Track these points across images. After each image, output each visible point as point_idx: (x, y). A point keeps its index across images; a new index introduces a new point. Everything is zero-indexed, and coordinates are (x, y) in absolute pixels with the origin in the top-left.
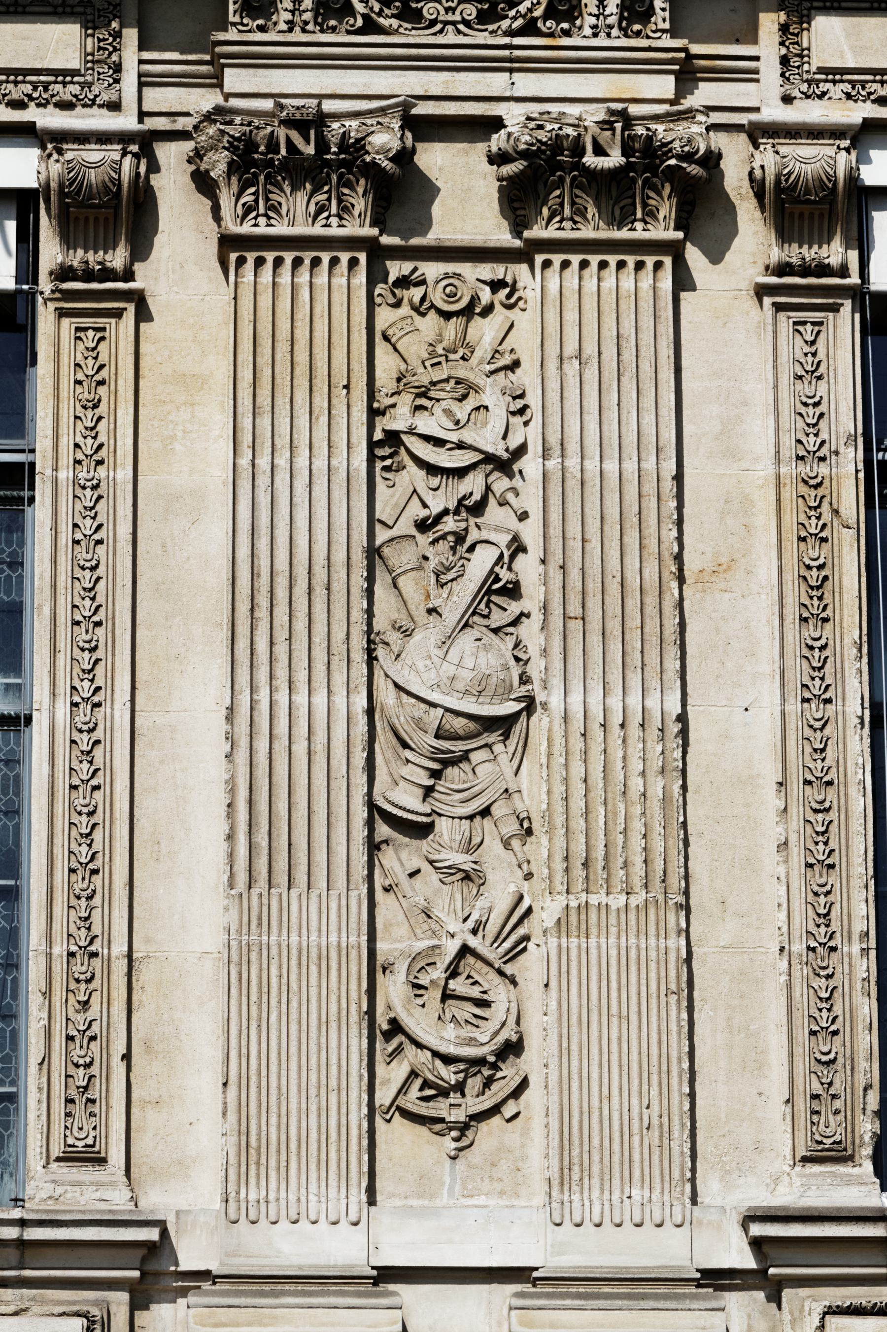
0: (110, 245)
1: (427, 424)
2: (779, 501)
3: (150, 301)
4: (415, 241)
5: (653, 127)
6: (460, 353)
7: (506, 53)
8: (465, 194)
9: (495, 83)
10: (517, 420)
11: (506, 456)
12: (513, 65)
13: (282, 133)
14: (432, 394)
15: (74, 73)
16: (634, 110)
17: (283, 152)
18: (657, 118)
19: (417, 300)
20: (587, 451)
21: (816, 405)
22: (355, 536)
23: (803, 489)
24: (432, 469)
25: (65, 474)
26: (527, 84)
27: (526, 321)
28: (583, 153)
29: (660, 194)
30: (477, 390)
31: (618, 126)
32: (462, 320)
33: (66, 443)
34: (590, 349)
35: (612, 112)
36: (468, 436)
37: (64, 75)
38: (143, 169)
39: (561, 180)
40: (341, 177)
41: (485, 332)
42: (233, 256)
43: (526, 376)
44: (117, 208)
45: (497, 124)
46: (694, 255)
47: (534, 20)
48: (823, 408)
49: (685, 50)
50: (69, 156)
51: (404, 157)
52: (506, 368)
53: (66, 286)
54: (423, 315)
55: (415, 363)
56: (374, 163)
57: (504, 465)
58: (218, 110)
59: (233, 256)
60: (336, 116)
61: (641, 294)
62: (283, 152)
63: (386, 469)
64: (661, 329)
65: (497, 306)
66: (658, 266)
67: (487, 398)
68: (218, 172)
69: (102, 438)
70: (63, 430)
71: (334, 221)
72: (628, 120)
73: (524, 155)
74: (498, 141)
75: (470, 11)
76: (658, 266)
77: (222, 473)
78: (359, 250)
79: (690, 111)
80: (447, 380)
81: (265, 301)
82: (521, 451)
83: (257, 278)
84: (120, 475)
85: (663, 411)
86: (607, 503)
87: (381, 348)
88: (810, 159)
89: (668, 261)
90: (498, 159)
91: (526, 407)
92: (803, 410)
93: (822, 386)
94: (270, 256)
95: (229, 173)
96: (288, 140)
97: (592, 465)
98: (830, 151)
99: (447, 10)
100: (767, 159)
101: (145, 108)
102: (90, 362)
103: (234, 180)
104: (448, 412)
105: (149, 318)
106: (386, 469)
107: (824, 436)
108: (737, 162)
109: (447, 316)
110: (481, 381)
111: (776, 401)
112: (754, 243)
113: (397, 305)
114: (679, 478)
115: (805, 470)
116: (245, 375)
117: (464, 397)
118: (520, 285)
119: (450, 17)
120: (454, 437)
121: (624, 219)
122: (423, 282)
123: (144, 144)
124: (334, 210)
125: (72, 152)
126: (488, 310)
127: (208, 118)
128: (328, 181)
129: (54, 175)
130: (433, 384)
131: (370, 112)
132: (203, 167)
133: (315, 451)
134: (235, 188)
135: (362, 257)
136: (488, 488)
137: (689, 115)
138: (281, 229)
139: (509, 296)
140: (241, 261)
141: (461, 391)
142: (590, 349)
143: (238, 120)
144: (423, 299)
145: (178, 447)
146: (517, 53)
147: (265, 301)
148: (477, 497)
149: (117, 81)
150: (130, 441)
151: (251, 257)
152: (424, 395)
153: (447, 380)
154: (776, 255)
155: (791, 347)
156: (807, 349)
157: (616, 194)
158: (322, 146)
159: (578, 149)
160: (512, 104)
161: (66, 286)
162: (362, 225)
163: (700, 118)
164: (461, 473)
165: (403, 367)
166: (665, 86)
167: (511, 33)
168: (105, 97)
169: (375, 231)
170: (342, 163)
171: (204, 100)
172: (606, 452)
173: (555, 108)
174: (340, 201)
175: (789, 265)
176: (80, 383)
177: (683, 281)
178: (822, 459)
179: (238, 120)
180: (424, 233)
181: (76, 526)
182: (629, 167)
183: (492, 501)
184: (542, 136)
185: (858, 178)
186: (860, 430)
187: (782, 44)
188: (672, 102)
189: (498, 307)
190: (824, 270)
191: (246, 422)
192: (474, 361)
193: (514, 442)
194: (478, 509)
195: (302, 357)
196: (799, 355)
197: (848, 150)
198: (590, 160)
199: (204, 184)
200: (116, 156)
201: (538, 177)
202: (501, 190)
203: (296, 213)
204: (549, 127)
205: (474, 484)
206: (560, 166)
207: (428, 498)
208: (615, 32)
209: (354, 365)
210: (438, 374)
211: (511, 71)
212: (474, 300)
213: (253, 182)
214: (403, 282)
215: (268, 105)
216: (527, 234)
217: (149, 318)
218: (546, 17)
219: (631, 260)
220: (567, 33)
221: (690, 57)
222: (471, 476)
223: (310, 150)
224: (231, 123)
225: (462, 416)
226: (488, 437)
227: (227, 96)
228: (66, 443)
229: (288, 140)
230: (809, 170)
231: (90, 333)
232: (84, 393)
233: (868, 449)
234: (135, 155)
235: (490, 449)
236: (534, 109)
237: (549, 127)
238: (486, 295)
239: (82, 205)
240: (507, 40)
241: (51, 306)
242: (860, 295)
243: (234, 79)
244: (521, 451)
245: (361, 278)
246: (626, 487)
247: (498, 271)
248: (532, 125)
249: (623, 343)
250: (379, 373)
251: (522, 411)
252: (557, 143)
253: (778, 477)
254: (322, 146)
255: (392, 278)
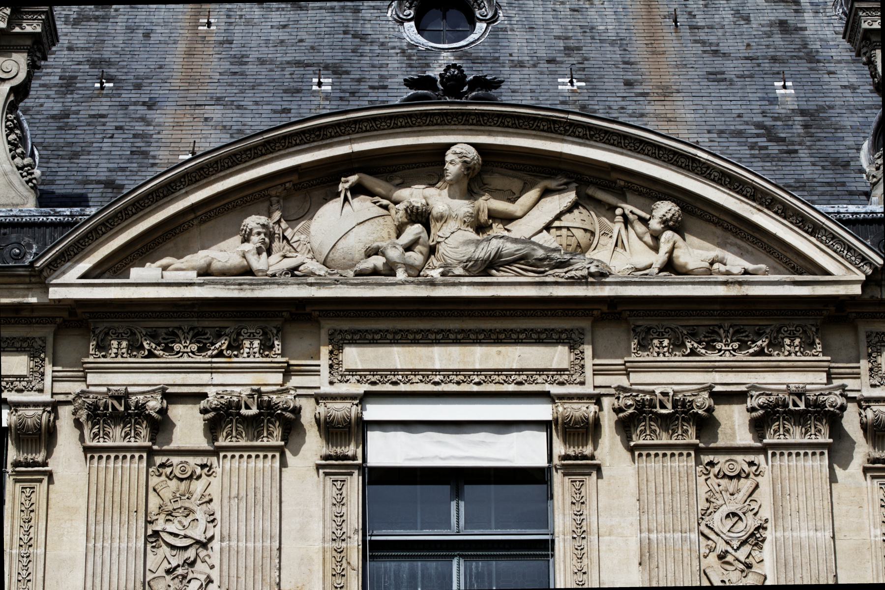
0: (38, 451)
1: (171, 528)
2: (324, 559)
3: (54, 475)
4: (165, 447)
5: (271, 396)
6: (187, 496)
7: (209, 365)
8: (188, 427)
9: (205, 378)
10: (211, 525)
11: (205, 541)
12: (212, 370)
13: (110, 402)
14: (174, 514)
15: (24, 377)
16: (263, 389)
17: (110, 410)
18: (273, 392)
19: (168, 473)
20: (240, 539)
21: (341, 516)
22: (138, 576)
23: (335, 554)
24: (173, 547)
25: (15, 551)
26: (218, 378)
27: (215, 482)
28: (241, 408)
29: (274, 426)
30: (193, 512)
31: (256, 396)
32: (188, 481)
33: (16, 537)
34: (243, 493)
35: (253, 390)
36: (188, 532)
37: (20, 378)
38: (52, 418)
39: (231, 420)
40: (136, 420)
41: (198, 487)
42: (89, 455)
43: (215, 506)
44: (40, 435)
45: (205, 396)
46: (288, 454)
47: (222, 350)
48: (344, 518)
49: (287, 362)
50: (19, 413)
51: (163, 412)
52: (206, 502)
53: (17, 469)
54: (171, 480)
55: (167, 501)
56: (149, 414)
57: (204, 545)
58: (83, 392)
59: (89, 455)
60: (134, 394)
61: (266, 469)
62: (110, 410)
63: (153, 547)
64: (274, 484)
65: (203, 475)
66: (273, 457)
67: (197, 516)
68: (83, 419)
69: (31, 535)
70: (15, 532)
71: (132, 439)
72: (260, 393)
73: (214, 409)
74: (203, 404)
75: (194, 347)
76: (273, 457)
77: (83, 550)
78: (143, 452)
79: (287, 389)
80: (180, 508)
81: (102, 475)
82: (212, 538)
83: (103, 466)
84: (39, 551)
85: (274, 520)
86: (248, 561)
87: (152, 495)
88: (340, 410)
89: (278, 455)
90: (204, 411)
91: (215, 519)
92: (335, 519)
93: (344, 509)
94: (105, 455)
95: (87, 420)
96: (112, 404)
97: (242, 544)
98: (349, 405)
99: (184, 347)
100: (322, 410)
101: (55, 391)
102: (28, 502)
103: (90, 423)
104: (180, 522)
105: (53, 483)
106: (153, 547)
107: (344, 530)
108: (309, 412)
109: (181, 480)
110: (195, 508)
111: (324, 515)
112: (314, 445)
113: (160, 475)
114: (280, 549)
115: (336, 545)
116: (93, 507)
117: (188, 515)
118: (214, 466)
119: (186, 350)
120: (182, 533)
121: (258, 436)
122: (172, 465)
123: (54, 407)
124: (133, 435)
125: (22, 411)
126: (199, 477)
127: (78, 396)
128: (130, 422)
129: (13, 421)
130: (174, 510)
131: (149, 392)
132: (77, 417)
133: (122, 540)
134: (90, 426)
135: (145, 455)
136: (197, 554)
137: (286, 391)
138: (109, 443)
139: (209, 471)
140: (92, 457)
141: (187, 512)
142: (243, 493)
143: (91, 396)
144: (171, 473)
145: (65, 538)
146: (214, 365)
147: (102, 475)
148: (192, 559)
149: (43, 380)
150: (44, 536)
151: (96, 456)
152: (170, 515)
153: (180, 508)
154: (325, 451)
155: (331, 491)
156: (338, 492)
157: (254, 425)
158: (128, 407)
159: (239, 407)
160: (211, 387)
161: (17, 469)
162: (145, 441)
163: (292, 392)
164: (185, 548)
165: (161, 502)
166: (278, 378)
167: (212, 356)
168: (37, 387)
169: (150, 444)
170: (136, 414)
171: (77, 387)
172: (249, 538)
173: (229, 389)
174: (135, 430)
175: (330, 455)
176: (22, 511)
177: (283, 464)
178: (343, 540)
179: (91, 396)
180: (169, 443)
181: (19, 574)
182: (260, 414)
183: (199, 561)
184: (223, 401)
185: (361, 418)
186: (360, 527)
187: (330, 359)
188: (281, 385)
189: (204, 476)
190: (346, 457)
191: (92, 528)
192: (193, 499)
193: (209, 535)
194: (192, 564)
195: (117, 499)
196: (334, 495)
197: (357, 405)
198: (243, 411)
199: (78, 424)
200: (40, 412)
201: (220, 419)
202: (205, 424)
203: (117, 437)
204: (226, 397)
205: (191, 554)
206: (231, 414)
207: (171, 560)
208: (257, 355)
209: (140, 502)
210: (176, 506)
211: (211, 373)
212: (193, 472)
213: (98, 423)
214: (163, 465)
215: (104, 389)
216: (216, 444)
217: (53, 483)
218: (227, 349)
219: (261, 454)
220: (236, 356)
221: (289, 365)
222: (190, 550)
223: (122, 409)
224: (88, 397)
225: (186, 523)
226: (198, 533)
227: (88, 386)
228: (16, 537)
229: (112, 404)
230: (339, 414)
231: (28, 490)
232: (25, 516)
233: (364, 535)
234: (49, 412)
235: (198, 538)
236: (221, 389)
237: (226, 397)
238: (198, 471)
239: (25, 434)
240: (210, 360)
241: (12, 478)
242: (363, 468)
243: (92, 378)
244: (212, 538)
245: (144, 464)
246: (257, 554)
247: (204, 460)
248: (219, 396)
249: (257, 490)
250: (150, 505)
251: (213, 521)
252: (230, 404)
253: (324, 548)
254: (128, 407)
255: (158, 464)
